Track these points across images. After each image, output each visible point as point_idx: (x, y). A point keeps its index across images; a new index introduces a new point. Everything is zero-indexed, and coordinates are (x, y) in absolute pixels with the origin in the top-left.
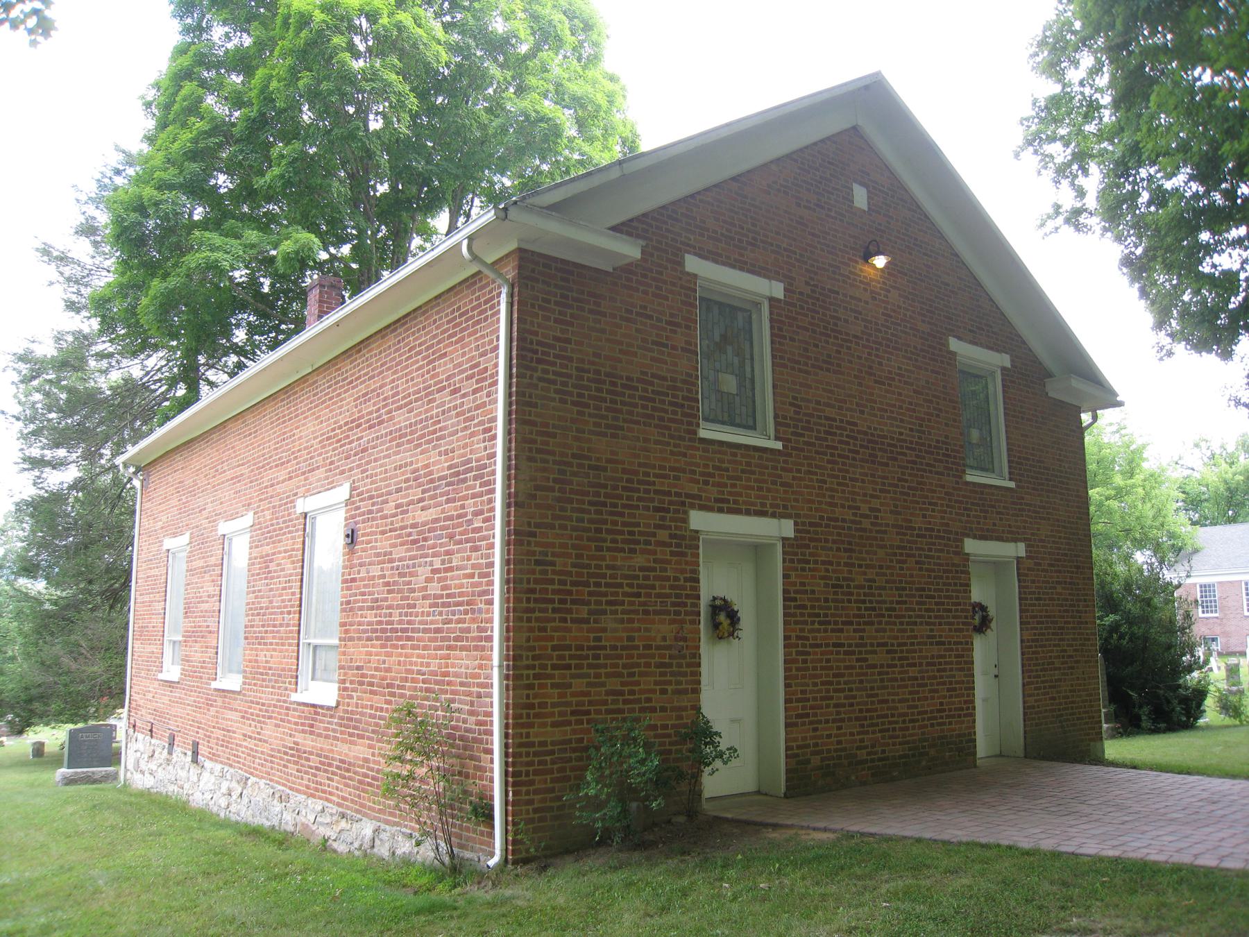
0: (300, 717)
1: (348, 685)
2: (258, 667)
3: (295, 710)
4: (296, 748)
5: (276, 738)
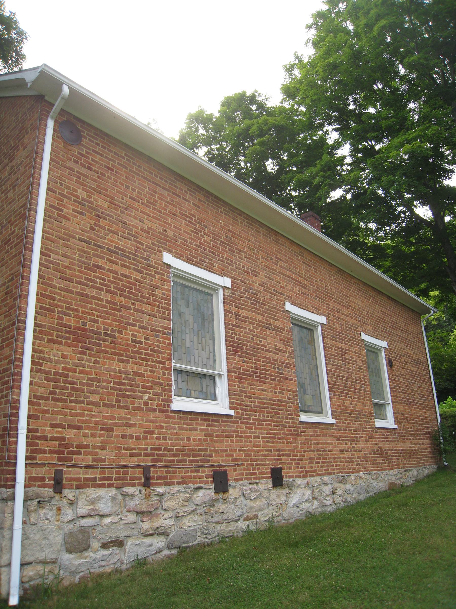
0: (380, 435)
1: (399, 420)
2: (347, 410)
3: (376, 432)
4: (381, 450)
5: (368, 447)
